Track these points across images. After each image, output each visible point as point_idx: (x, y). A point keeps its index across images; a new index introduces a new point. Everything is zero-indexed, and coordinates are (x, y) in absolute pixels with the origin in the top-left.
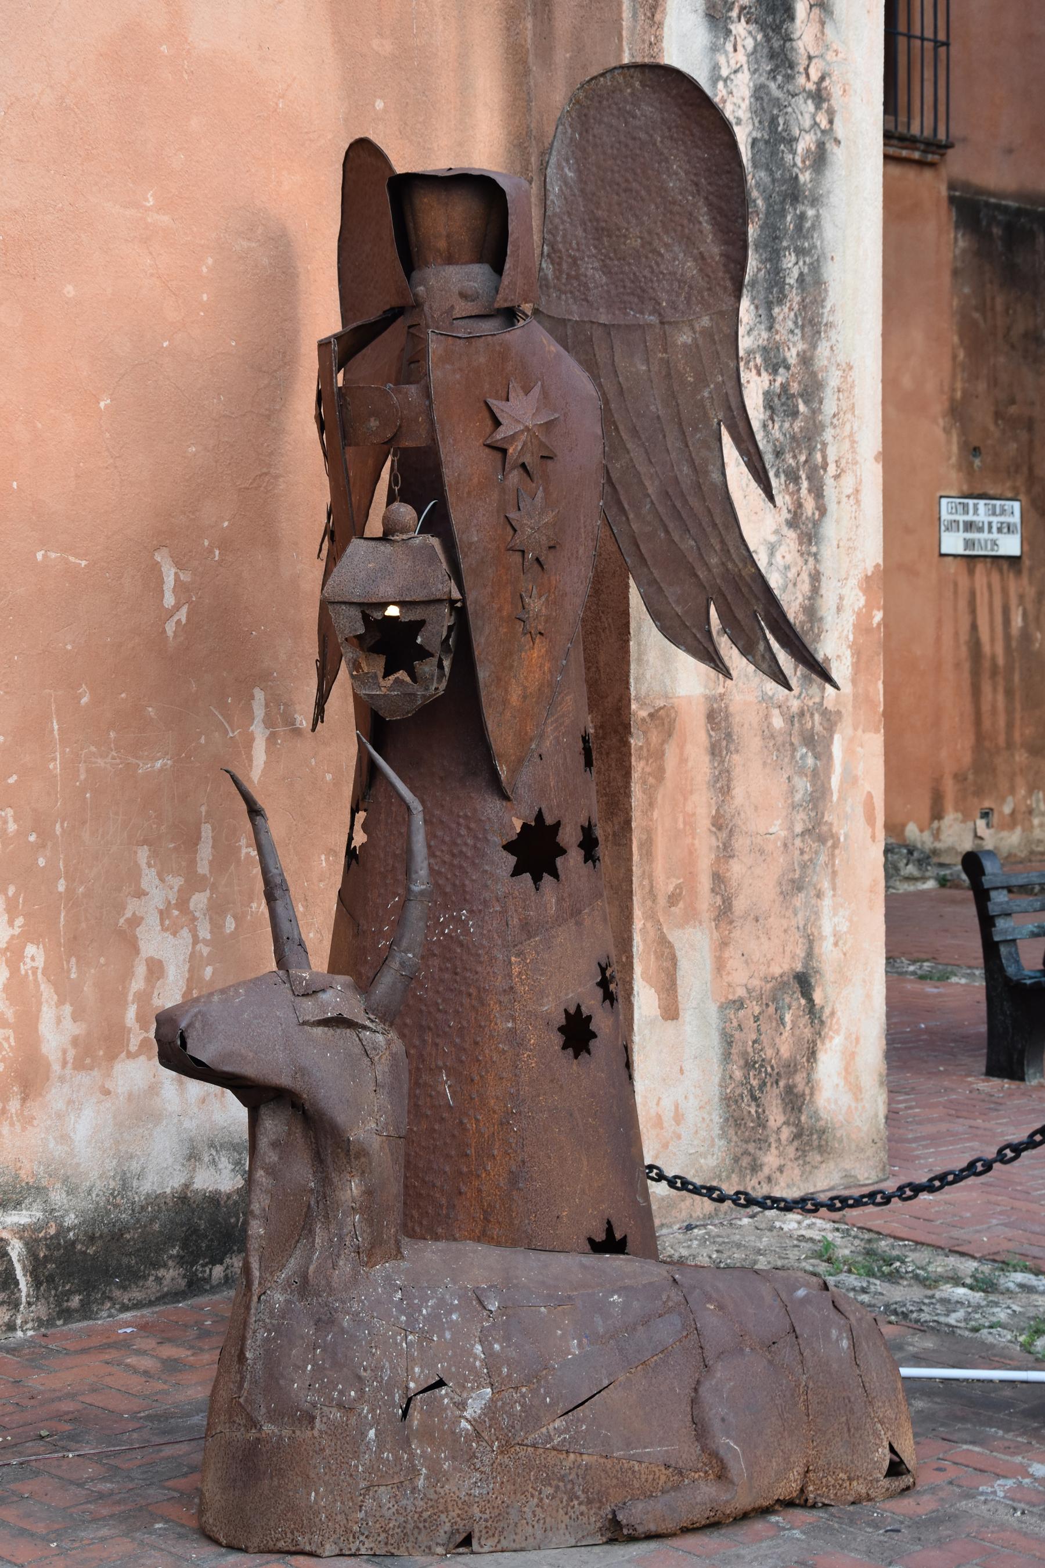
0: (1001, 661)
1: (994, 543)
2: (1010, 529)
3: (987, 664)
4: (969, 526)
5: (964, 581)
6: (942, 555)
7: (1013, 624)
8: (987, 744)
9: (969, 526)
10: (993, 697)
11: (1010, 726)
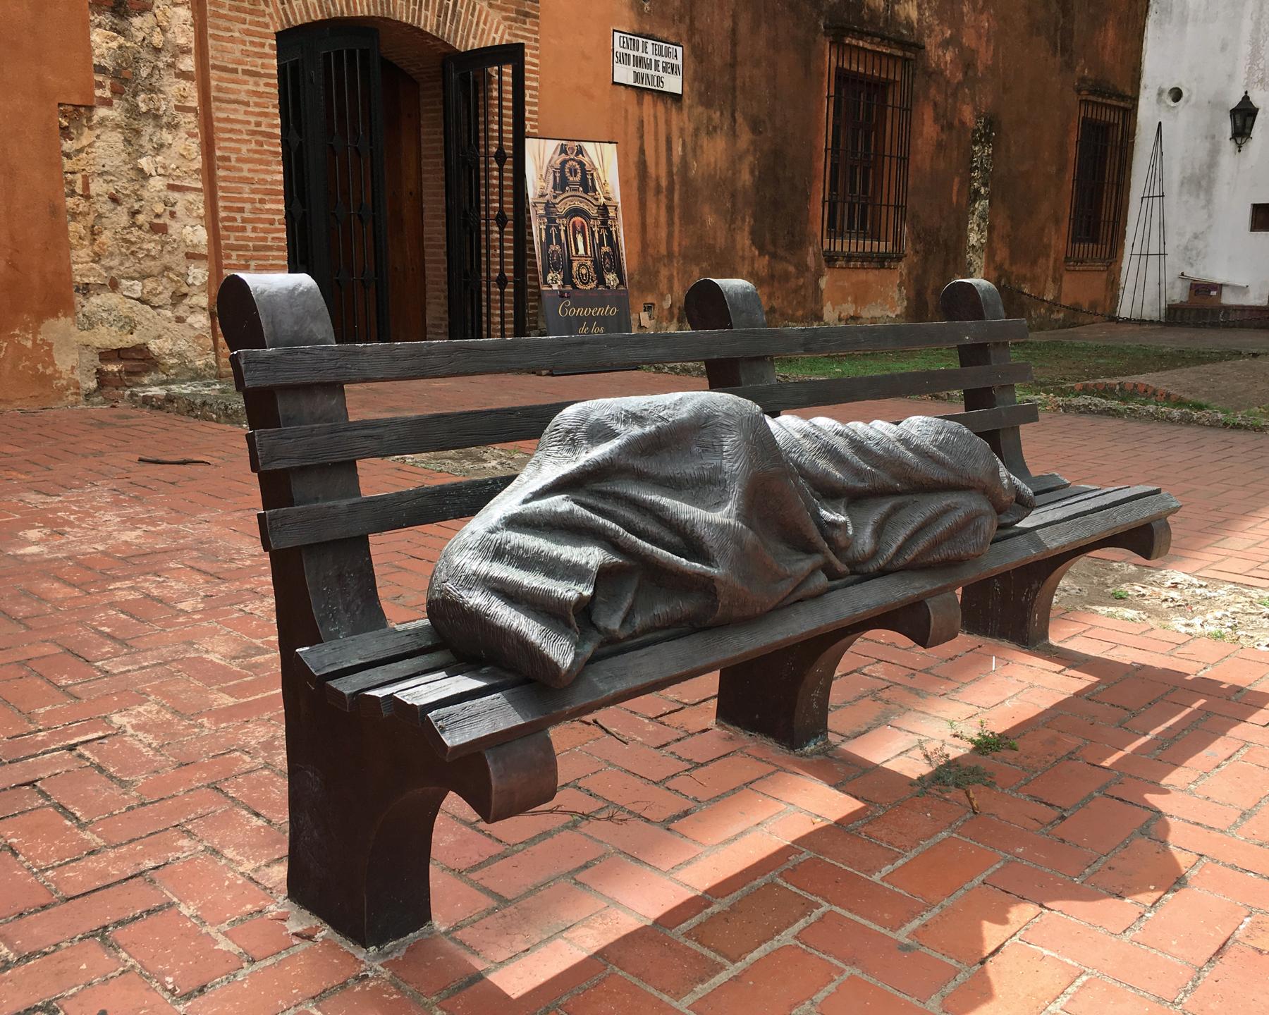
0: (664, 183)
1: (660, 80)
2: (673, 69)
3: (652, 184)
4: (639, 61)
5: (633, 109)
6: (614, 83)
7: (674, 153)
8: (651, 251)
9: (639, 61)
10: (657, 211)
11: (670, 236)
